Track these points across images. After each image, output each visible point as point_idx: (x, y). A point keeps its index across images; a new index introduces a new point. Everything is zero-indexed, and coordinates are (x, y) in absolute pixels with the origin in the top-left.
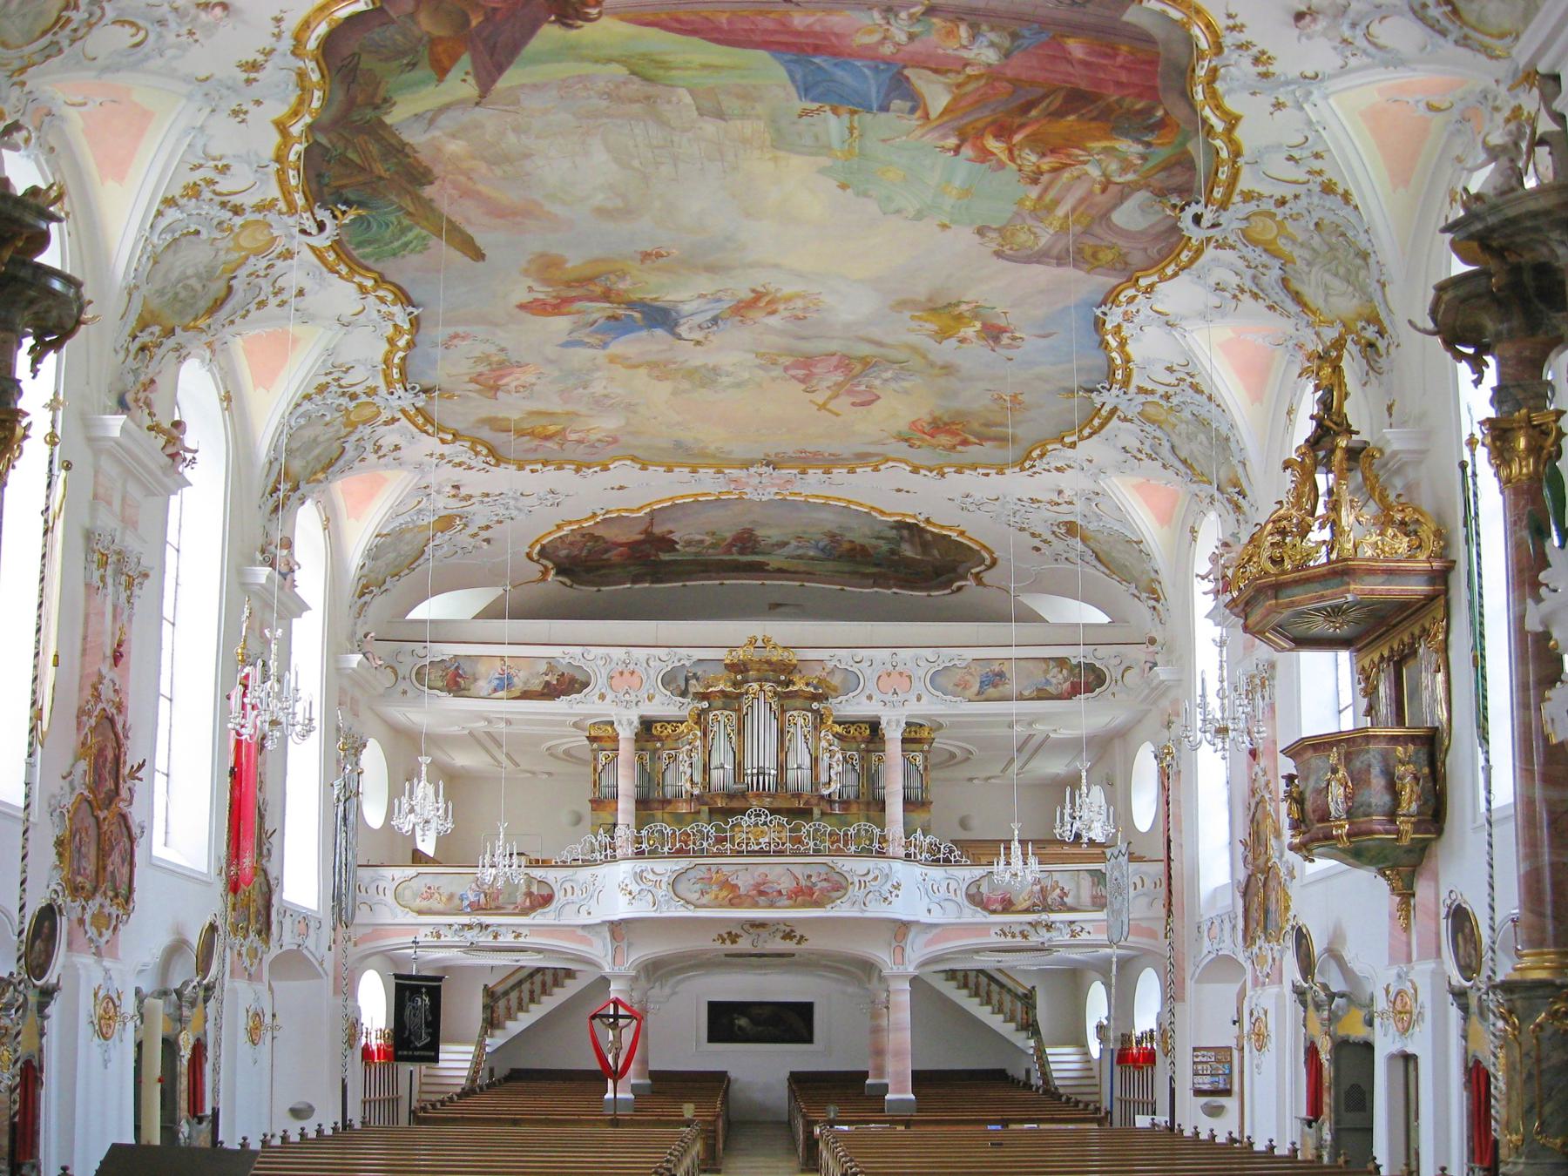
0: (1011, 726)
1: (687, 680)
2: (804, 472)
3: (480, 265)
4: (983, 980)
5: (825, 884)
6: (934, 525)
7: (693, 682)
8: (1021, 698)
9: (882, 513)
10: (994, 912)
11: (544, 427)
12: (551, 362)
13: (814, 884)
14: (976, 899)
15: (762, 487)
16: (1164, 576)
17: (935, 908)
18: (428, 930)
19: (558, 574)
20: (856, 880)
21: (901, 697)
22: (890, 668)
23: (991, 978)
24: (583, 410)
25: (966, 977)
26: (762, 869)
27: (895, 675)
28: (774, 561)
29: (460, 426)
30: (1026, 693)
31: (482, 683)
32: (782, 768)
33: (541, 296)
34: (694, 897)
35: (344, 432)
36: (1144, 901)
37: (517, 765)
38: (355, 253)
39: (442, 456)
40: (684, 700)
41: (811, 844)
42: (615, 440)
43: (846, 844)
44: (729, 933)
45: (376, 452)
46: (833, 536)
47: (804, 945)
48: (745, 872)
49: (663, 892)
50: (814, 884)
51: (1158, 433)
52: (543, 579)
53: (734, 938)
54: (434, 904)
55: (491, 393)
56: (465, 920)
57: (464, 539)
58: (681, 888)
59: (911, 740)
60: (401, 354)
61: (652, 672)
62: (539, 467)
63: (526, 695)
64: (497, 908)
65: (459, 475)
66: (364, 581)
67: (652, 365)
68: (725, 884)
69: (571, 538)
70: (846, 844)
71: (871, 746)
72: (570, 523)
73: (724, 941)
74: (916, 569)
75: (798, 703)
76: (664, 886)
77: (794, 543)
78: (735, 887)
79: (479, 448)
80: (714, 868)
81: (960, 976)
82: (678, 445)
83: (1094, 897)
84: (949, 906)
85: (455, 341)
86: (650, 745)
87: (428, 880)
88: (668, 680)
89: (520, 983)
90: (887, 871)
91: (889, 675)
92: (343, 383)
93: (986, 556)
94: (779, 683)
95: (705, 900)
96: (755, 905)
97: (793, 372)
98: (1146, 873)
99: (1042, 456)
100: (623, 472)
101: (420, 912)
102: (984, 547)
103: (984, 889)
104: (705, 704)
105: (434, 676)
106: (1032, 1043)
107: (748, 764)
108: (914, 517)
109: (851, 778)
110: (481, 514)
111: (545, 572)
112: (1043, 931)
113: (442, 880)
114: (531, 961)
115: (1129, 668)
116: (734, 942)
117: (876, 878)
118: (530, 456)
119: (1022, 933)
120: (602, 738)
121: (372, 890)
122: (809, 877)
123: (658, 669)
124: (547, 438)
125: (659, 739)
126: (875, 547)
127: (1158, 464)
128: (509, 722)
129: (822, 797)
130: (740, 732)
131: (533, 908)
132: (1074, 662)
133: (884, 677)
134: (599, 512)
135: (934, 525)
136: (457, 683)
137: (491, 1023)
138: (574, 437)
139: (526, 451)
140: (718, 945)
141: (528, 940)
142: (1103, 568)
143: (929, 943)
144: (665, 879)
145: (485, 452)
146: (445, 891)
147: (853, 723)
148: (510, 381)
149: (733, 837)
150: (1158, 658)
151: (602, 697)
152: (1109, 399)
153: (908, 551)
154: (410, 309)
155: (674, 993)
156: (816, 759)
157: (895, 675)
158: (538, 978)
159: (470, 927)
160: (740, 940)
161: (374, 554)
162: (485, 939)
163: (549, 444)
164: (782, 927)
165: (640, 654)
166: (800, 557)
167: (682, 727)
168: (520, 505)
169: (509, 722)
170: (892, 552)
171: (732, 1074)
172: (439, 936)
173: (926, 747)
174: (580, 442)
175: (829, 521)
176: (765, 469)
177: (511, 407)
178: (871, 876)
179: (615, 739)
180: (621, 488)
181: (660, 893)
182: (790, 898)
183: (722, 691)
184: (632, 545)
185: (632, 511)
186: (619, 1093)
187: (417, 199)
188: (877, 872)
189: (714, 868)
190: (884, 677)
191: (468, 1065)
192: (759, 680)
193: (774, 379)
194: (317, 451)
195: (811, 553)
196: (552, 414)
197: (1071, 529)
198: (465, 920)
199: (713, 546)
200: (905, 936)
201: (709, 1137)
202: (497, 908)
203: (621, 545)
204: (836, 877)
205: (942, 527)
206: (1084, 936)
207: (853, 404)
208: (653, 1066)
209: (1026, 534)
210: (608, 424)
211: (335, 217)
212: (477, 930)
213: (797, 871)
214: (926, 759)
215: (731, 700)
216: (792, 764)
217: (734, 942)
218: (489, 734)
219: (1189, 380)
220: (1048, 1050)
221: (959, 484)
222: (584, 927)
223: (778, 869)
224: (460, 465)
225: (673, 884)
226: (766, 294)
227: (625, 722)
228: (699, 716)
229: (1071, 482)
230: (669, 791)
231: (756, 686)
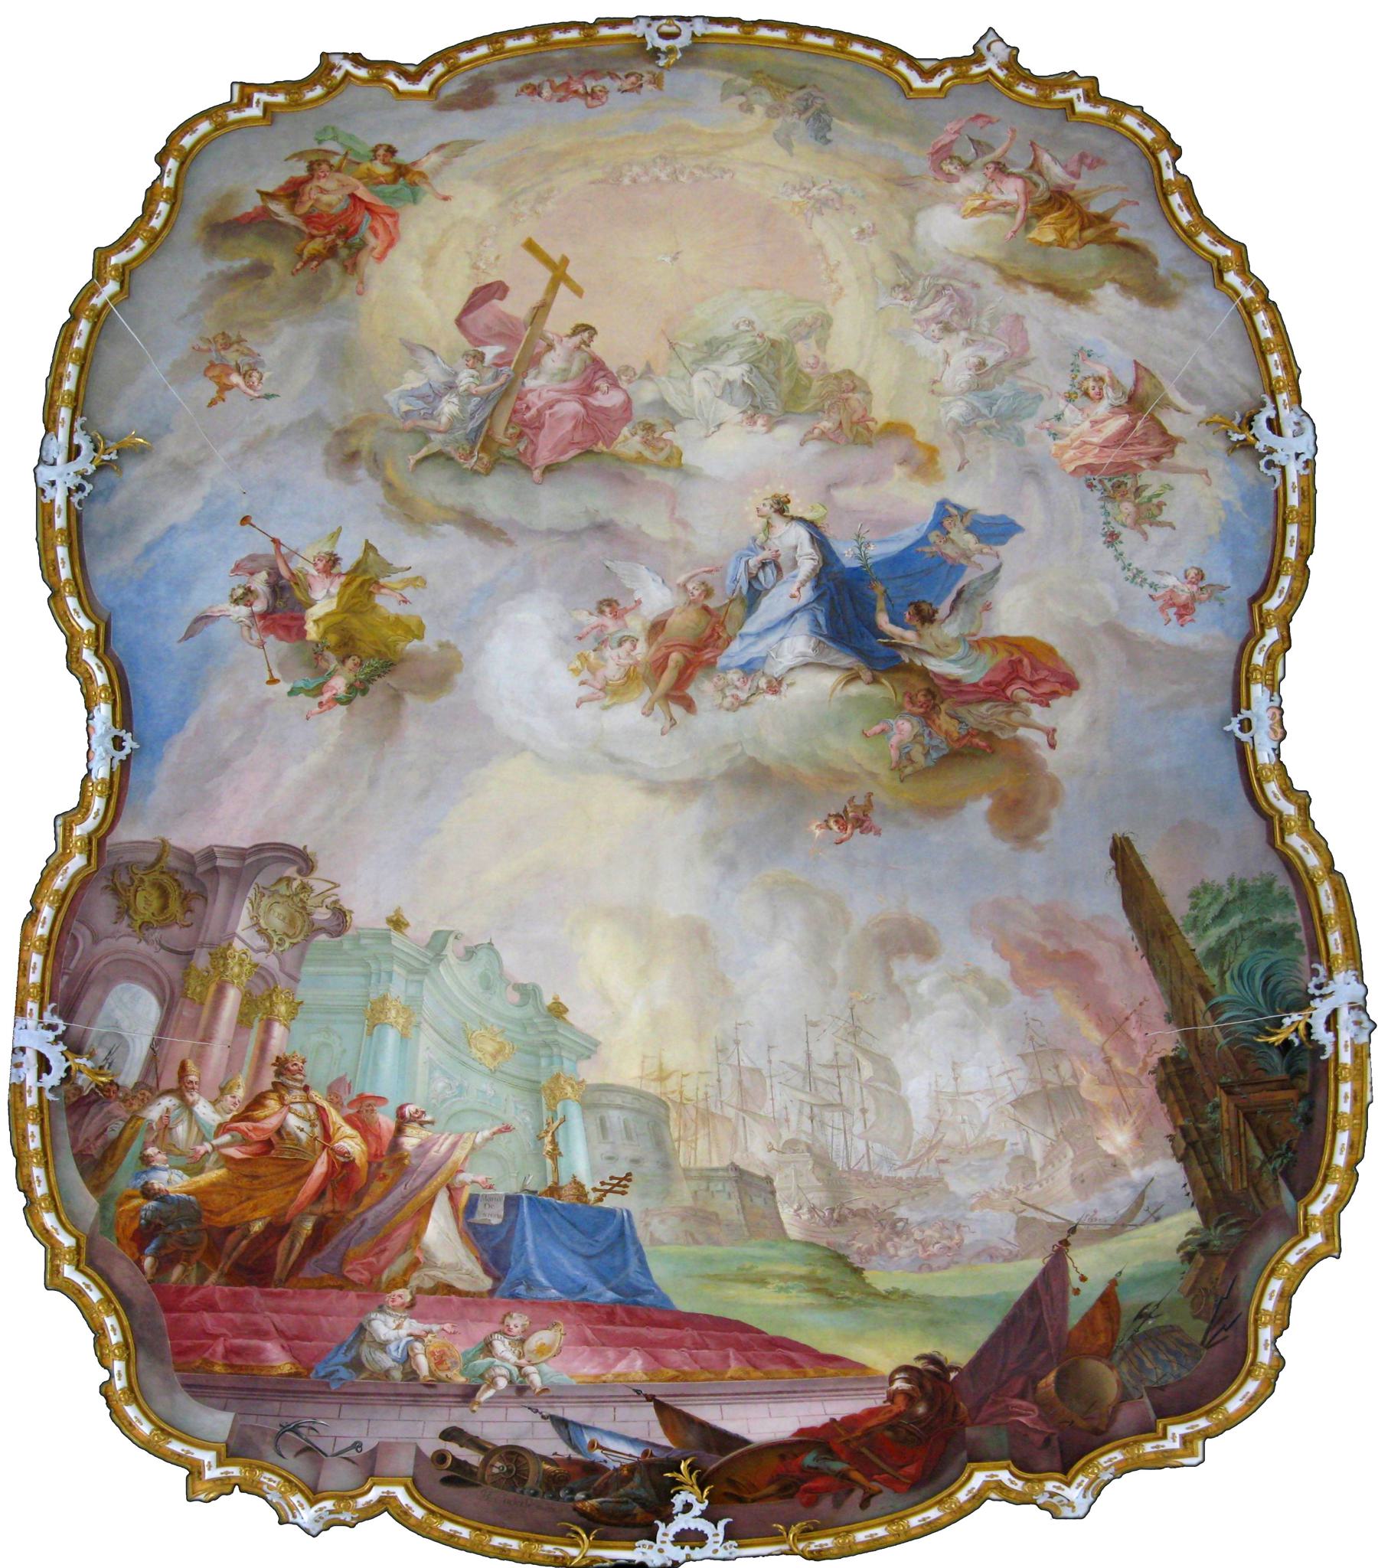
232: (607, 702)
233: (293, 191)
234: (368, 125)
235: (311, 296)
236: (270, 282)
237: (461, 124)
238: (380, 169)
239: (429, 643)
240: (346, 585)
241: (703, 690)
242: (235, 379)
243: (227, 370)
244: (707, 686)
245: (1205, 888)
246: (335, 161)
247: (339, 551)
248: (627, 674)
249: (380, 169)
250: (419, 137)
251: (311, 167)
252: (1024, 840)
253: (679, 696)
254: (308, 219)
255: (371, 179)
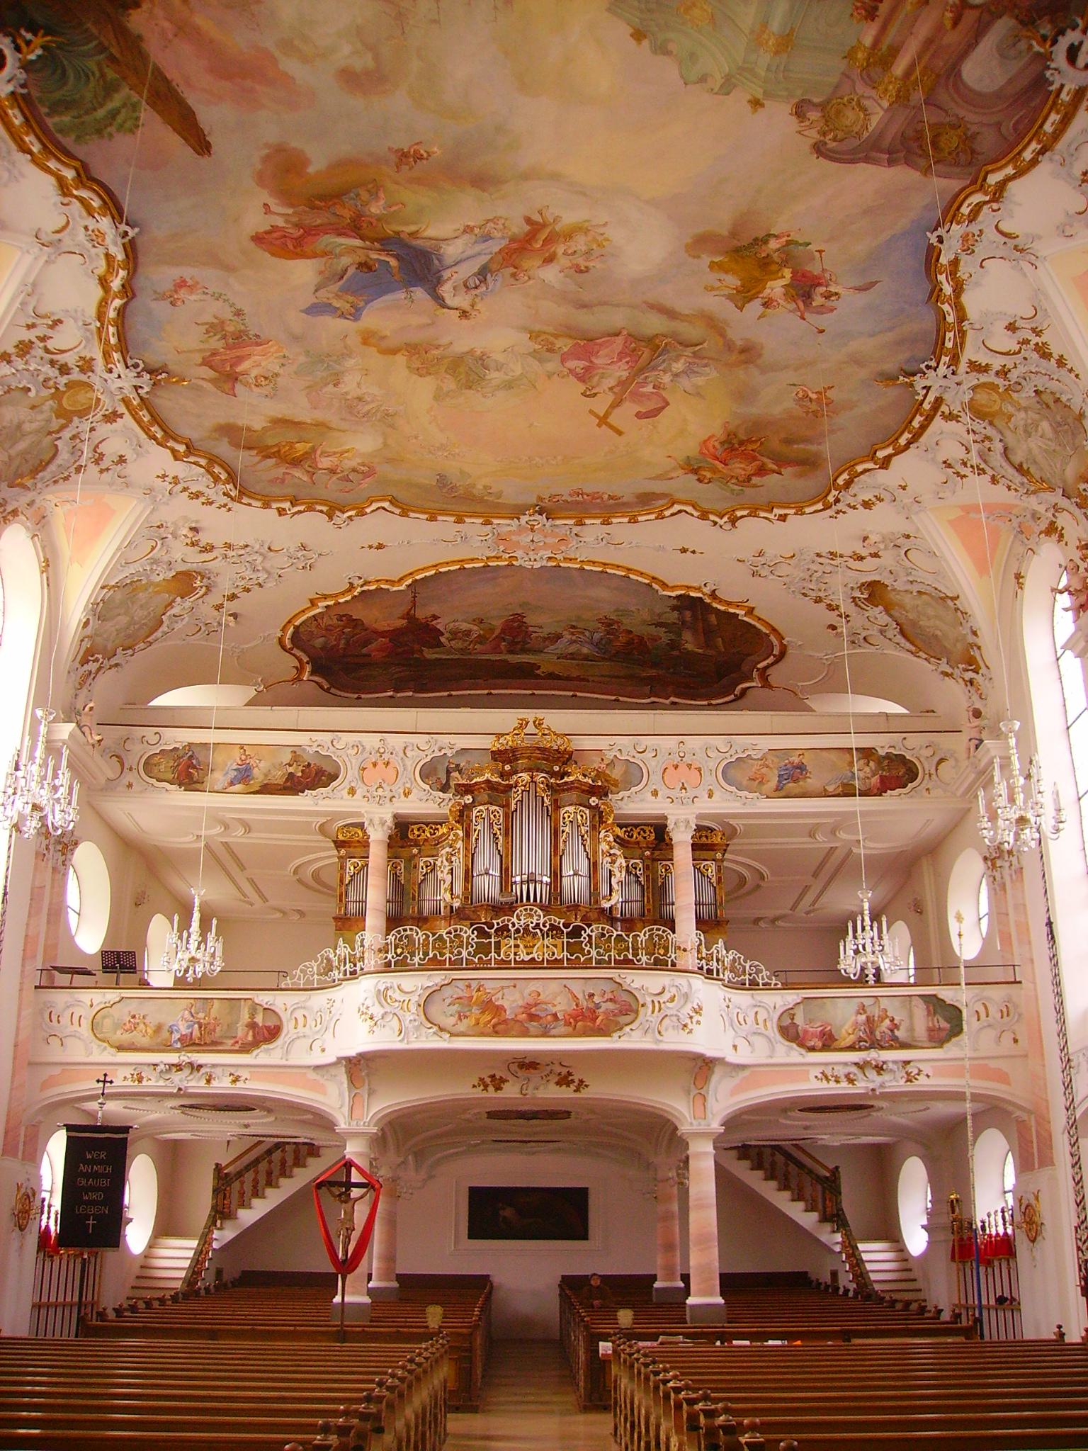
0: (811, 835)
1: (448, 772)
2: (580, 523)
3: (204, 161)
4: (780, 1158)
5: (610, 1006)
6: (721, 601)
7: (456, 774)
8: (825, 794)
9: (664, 585)
10: (812, 1049)
11: (291, 445)
12: (296, 338)
13: (598, 1006)
14: (790, 1032)
15: (534, 546)
16: (985, 639)
17: (742, 1044)
18: (128, 1072)
19: (313, 673)
20: (649, 1000)
21: (691, 793)
22: (680, 765)
23: (788, 1156)
24: (334, 421)
25: (760, 1155)
26: (533, 986)
27: (683, 768)
28: (546, 661)
29: (194, 435)
30: (830, 789)
31: (218, 775)
32: (556, 875)
33: (280, 222)
34: (449, 1022)
35: (56, 424)
36: (991, 1034)
37: (265, 900)
38: (50, 122)
39: (176, 480)
40: (446, 796)
41: (594, 953)
42: (370, 473)
43: (636, 955)
44: (493, 1077)
45: (97, 462)
46: (609, 624)
47: (584, 1094)
48: (511, 989)
49: (412, 1015)
50: (598, 1006)
51: (990, 431)
52: (298, 679)
53: (498, 1083)
54: (138, 1038)
55: (227, 387)
56: (173, 1058)
57: (206, 610)
58: (434, 1011)
59: (704, 844)
60: (118, 303)
61: (409, 763)
62: (287, 505)
63: (267, 789)
64: (214, 1043)
65: (195, 511)
66: (87, 644)
67: (413, 349)
68: (489, 1006)
69: (326, 622)
70: (636, 955)
71: (657, 853)
72: (325, 597)
73: (486, 1087)
74: (699, 655)
75: (573, 796)
76: (413, 1008)
77: (567, 636)
78: (500, 1009)
79: (217, 470)
80: (474, 984)
81: (753, 1153)
82: (442, 481)
83: (930, 1030)
84: (759, 1042)
85: (183, 293)
86: (405, 852)
87: (133, 1007)
88: (427, 773)
89: (257, 1161)
90: (685, 989)
91: (676, 767)
92: (51, 345)
93: (775, 642)
94: (552, 774)
95: (462, 1027)
96: (525, 1033)
97: (572, 364)
98: (988, 999)
99: (848, 484)
100: (380, 524)
101: (120, 1048)
102: (774, 630)
103: (799, 1020)
104: (468, 799)
105: (165, 766)
106: (838, 1237)
107: (516, 869)
108: (698, 589)
109: (634, 892)
110: (227, 577)
111: (300, 670)
112: (872, 1074)
113: (148, 1008)
114: (261, 1124)
115: (942, 760)
116: (498, 1088)
117: (672, 999)
118: (276, 490)
119: (847, 1076)
120: (350, 842)
121: (65, 1020)
122: (591, 995)
123: (414, 761)
124: (296, 462)
125: (416, 844)
126: (655, 639)
127: (987, 478)
128: (248, 827)
129: (603, 910)
130: (508, 832)
131: (255, 1044)
132: (882, 752)
133: (671, 770)
134: (357, 582)
135: (721, 601)
136: (190, 775)
137: (221, 1213)
138: (325, 463)
139: (273, 481)
140: (478, 1093)
141: (249, 1085)
142: (908, 646)
143: (733, 1092)
144: (415, 998)
145: (224, 476)
146: (153, 1020)
147: (636, 826)
148: (252, 366)
149: (498, 944)
150: (983, 736)
151: (352, 791)
152: (934, 381)
153: (690, 643)
154: (123, 227)
155: (431, 1177)
156: (595, 864)
157: (683, 768)
158: (277, 1156)
159: (179, 1067)
160: (506, 1086)
161: (101, 611)
162: (196, 1084)
163: (297, 473)
164: (558, 1069)
165: (396, 741)
166: (572, 656)
167: (443, 830)
168: (268, 565)
169: (248, 827)
170: (673, 645)
171: (496, 1280)
172: (140, 1080)
173: (719, 855)
174: (332, 471)
175: (604, 599)
176: (537, 517)
177: (253, 410)
178: (666, 996)
179: (366, 845)
180: (380, 546)
181: (409, 1017)
182: (568, 1024)
183: (488, 781)
184: (395, 635)
185: (392, 582)
186: (352, 1294)
187: (122, 33)
188: (674, 990)
189: (474, 984)
190: (671, 770)
191: (187, 1264)
192: (529, 770)
193: (549, 376)
194: (22, 445)
195: (585, 650)
196: (297, 424)
197: (874, 593)
198: (173, 1058)
199: (481, 639)
200: (707, 1080)
201: (461, 1353)
202: (214, 1043)
203: (382, 634)
204: (625, 997)
205: (729, 604)
206: (922, 1080)
207: (639, 415)
208: (400, 1270)
209: (823, 605)
210: (362, 444)
211: (18, 49)
212: (187, 1071)
213: (577, 988)
214: (719, 869)
215: (498, 792)
216: (567, 871)
217: (498, 1088)
218: (226, 844)
219: (1035, 340)
220: (861, 1246)
221: (757, 533)
222: (317, 1068)
223: (554, 986)
224: (197, 495)
225: (425, 1005)
226: (544, 226)
227: (376, 821)
228: (461, 812)
229: (882, 521)
230: (426, 907)
231: (526, 777)
232: (586, 224)
233: (762, 471)
234: (710, 494)
235: (758, 426)
236: (783, 435)
237: (658, 487)
238: (708, 475)
239: (706, 259)
240: (759, 292)
241: (519, 228)
242: (814, 396)
243: (819, 401)
244: (515, 230)
245: (132, 131)
246: (734, 481)
247: (761, 309)
248: (571, 237)
249: (708, 475)
250: (685, 484)
251: (749, 479)
252: (280, 149)
253: (535, 227)
254: (755, 459)
255: (714, 470)
